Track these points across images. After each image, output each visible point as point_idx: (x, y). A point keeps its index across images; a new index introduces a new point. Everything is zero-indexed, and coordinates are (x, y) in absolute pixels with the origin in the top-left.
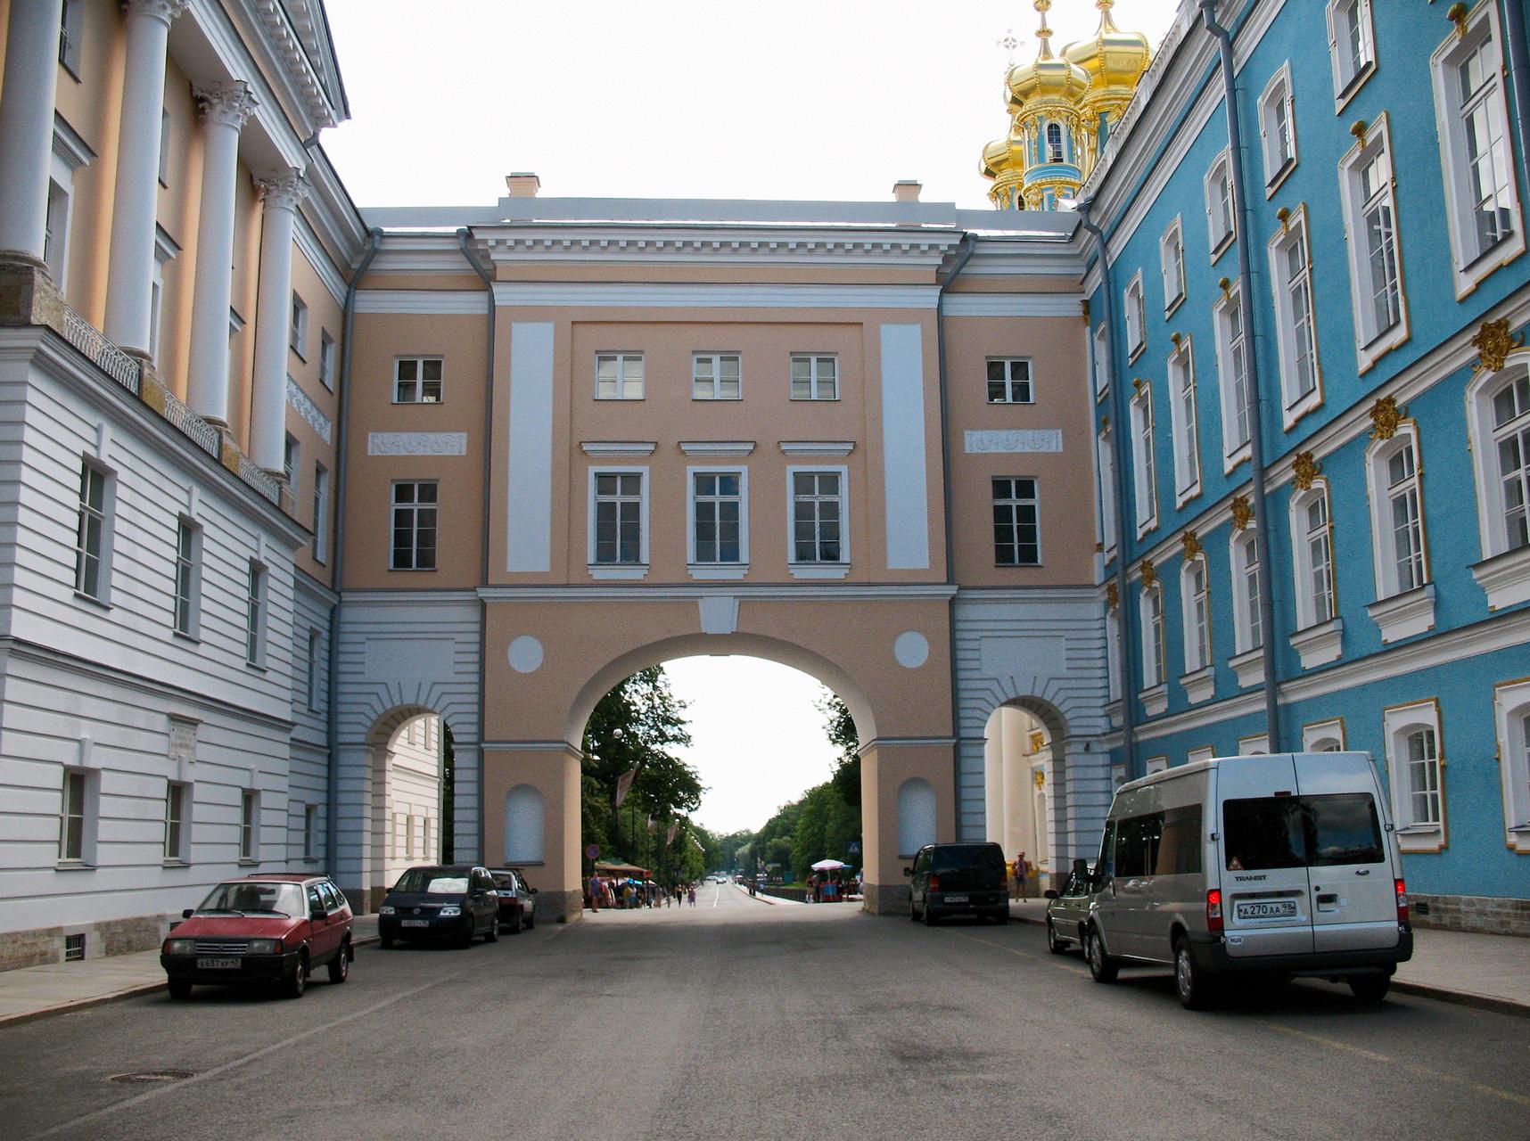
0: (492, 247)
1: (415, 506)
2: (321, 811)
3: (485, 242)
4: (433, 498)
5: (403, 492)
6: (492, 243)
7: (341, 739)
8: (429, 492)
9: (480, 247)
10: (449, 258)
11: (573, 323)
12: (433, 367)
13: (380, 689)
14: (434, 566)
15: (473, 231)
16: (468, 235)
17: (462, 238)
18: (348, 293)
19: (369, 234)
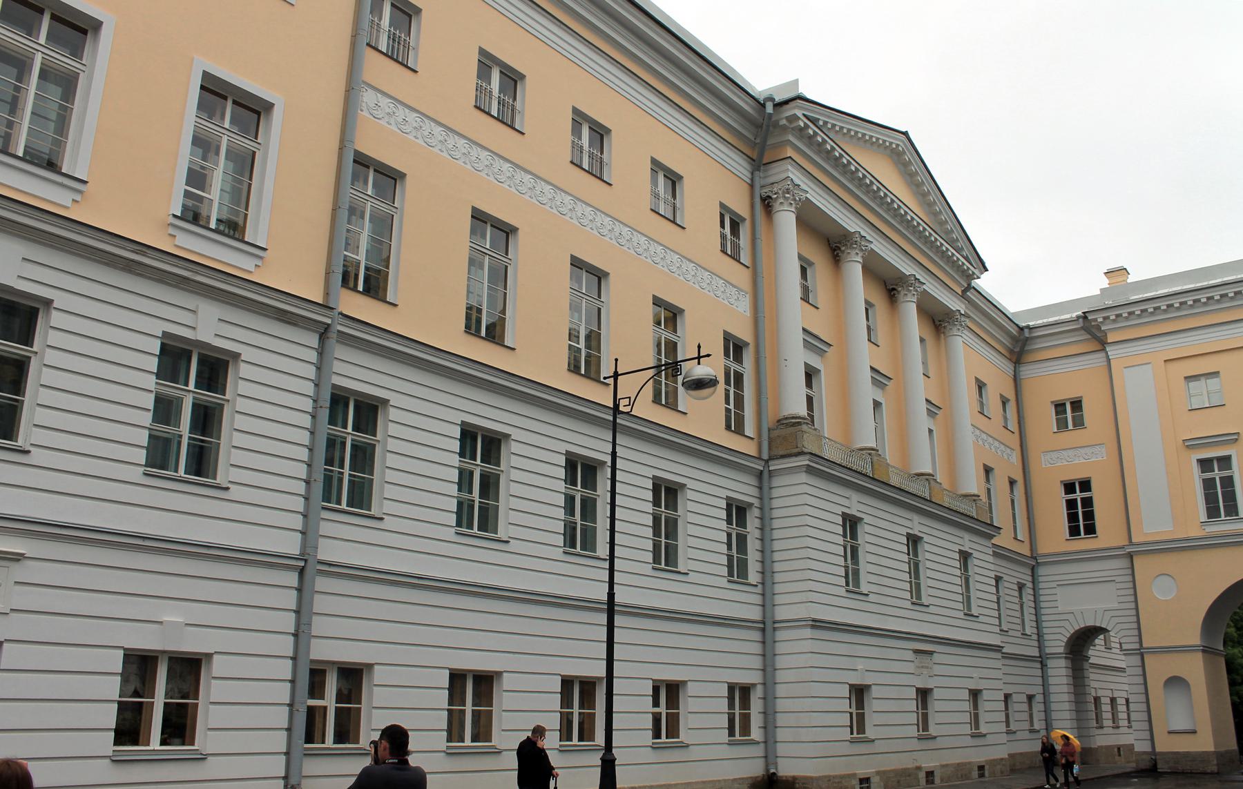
0: (1101, 322)
1: (1078, 495)
2: (1039, 698)
3: (1095, 320)
4: (1089, 489)
5: (1069, 487)
6: (1100, 320)
7: (1048, 650)
8: (1086, 485)
9: (1093, 324)
10: (1077, 333)
11: (1165, 361)
12: (1077, 405)
13: (1070, 617)
14: (1095, 534)
15: (1087, 314)
16: (1085, 316)
17: (1081, 320)
18: (1015, 367)
19: (1021, 329)
